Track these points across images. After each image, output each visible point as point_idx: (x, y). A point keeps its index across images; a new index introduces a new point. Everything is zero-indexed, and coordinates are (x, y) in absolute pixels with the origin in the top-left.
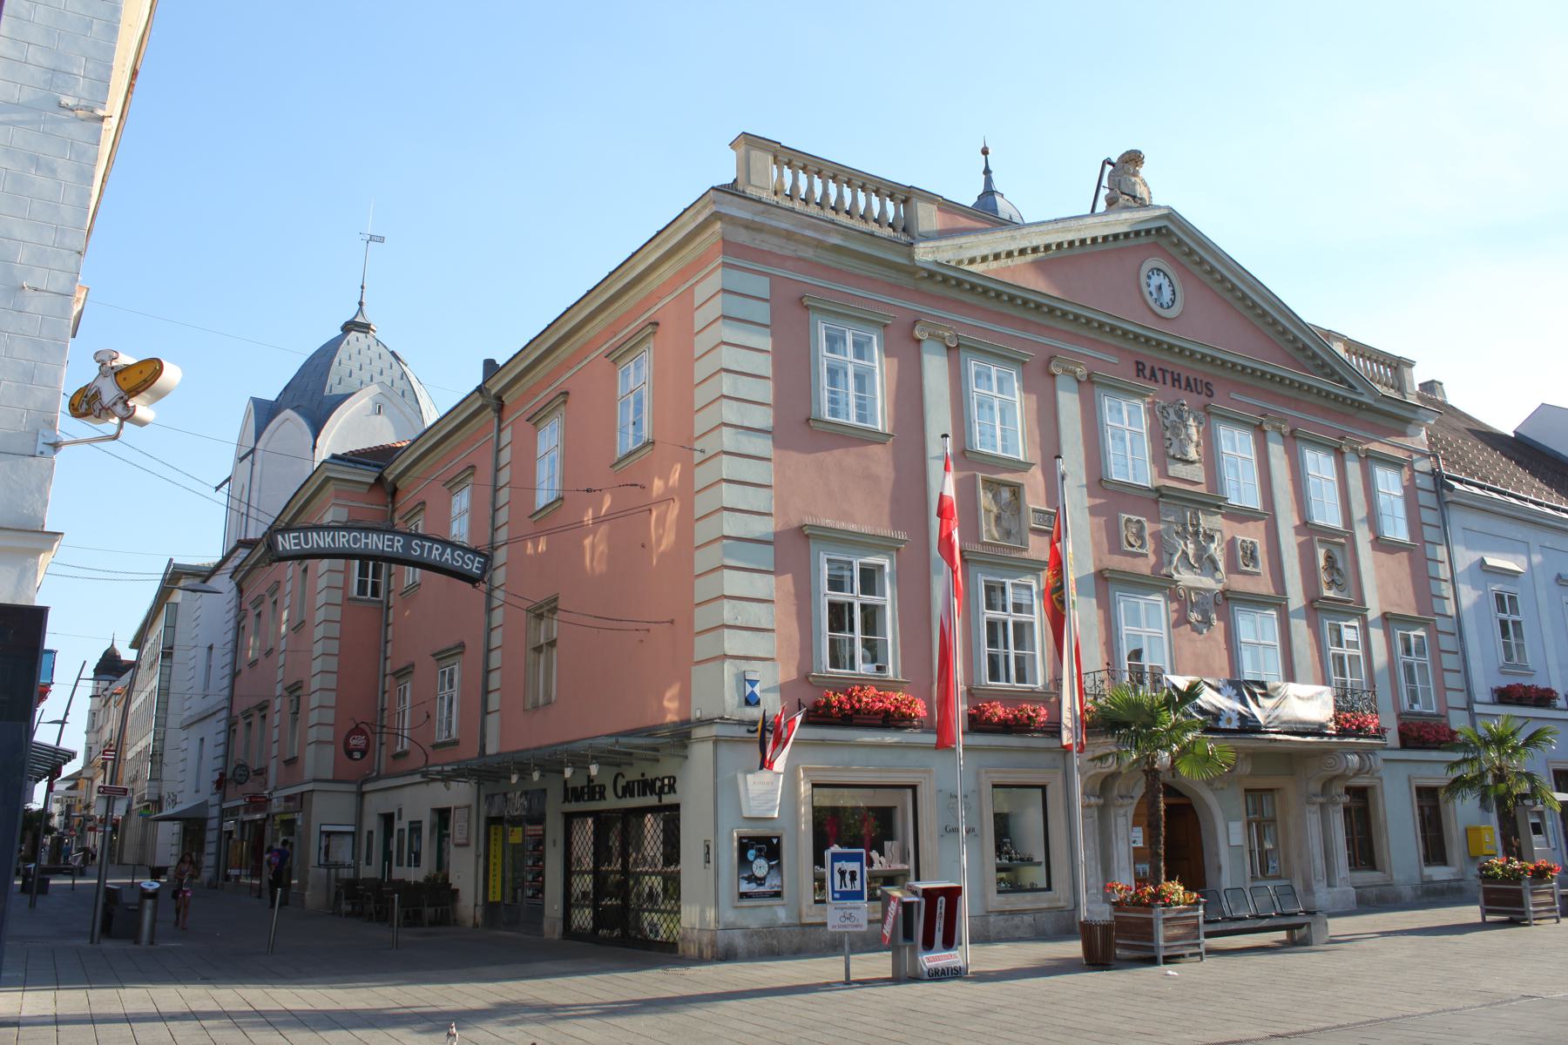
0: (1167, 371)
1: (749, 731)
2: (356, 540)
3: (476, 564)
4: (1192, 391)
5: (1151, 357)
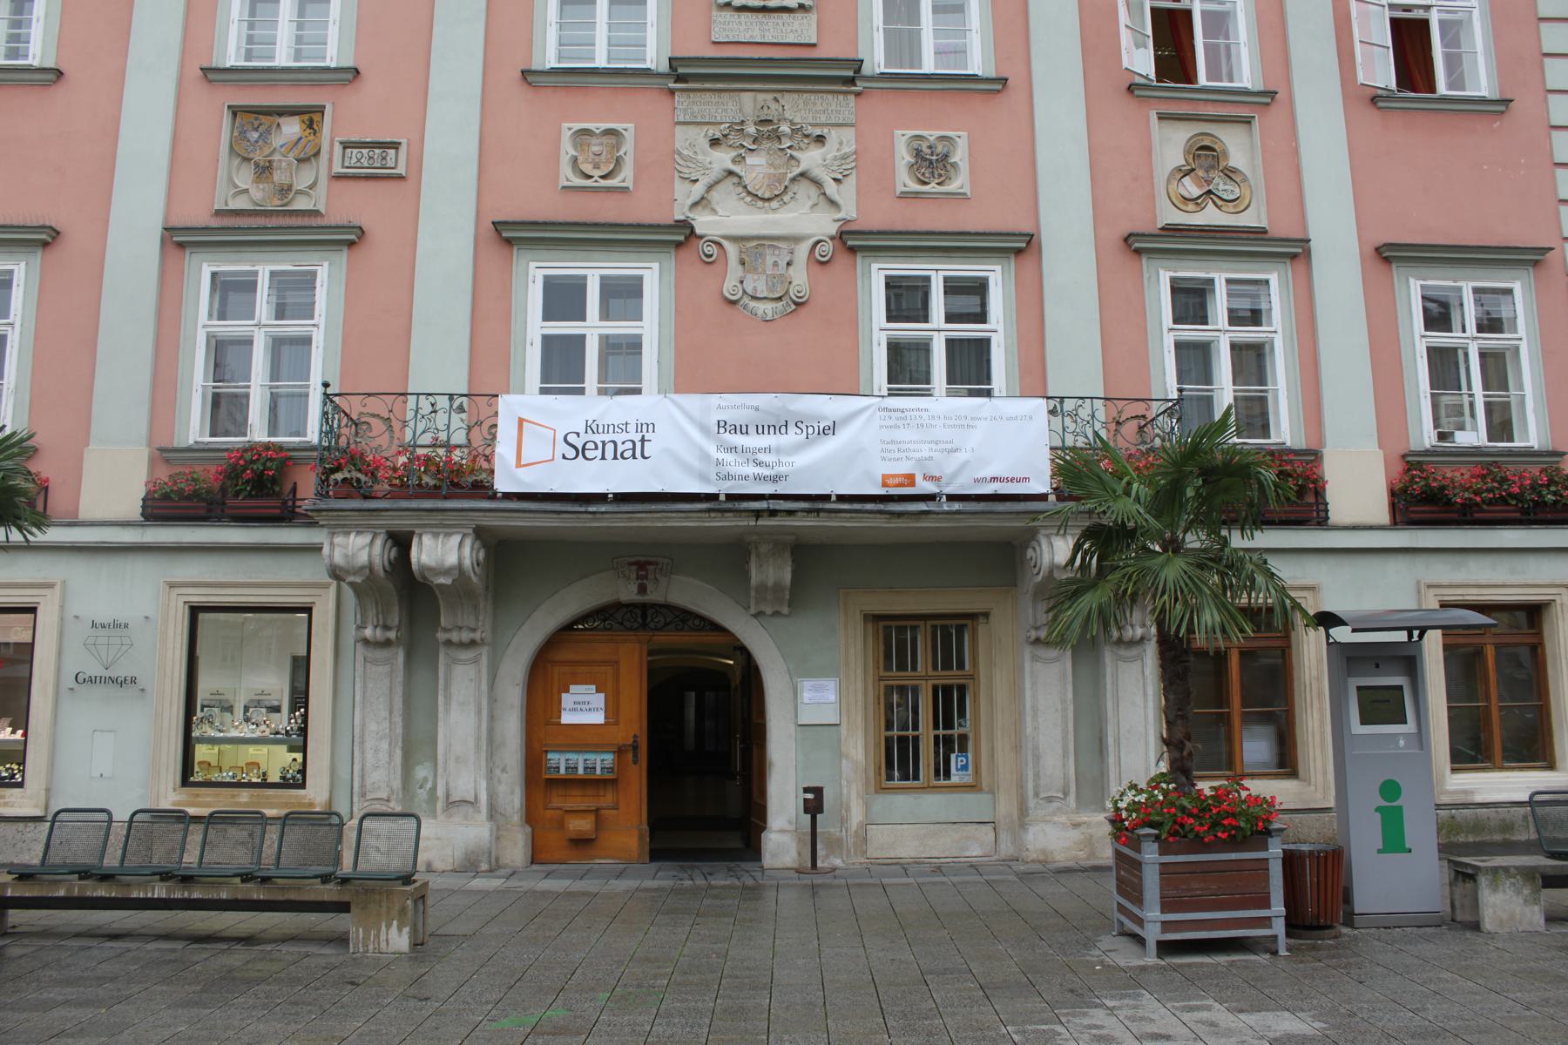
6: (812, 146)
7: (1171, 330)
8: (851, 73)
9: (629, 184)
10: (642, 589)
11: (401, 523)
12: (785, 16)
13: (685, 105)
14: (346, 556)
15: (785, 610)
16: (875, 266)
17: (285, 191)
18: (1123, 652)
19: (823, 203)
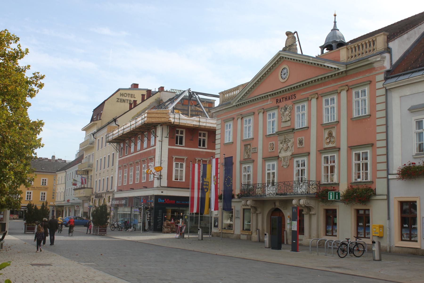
0: (284, 98)
5: (279, 96)
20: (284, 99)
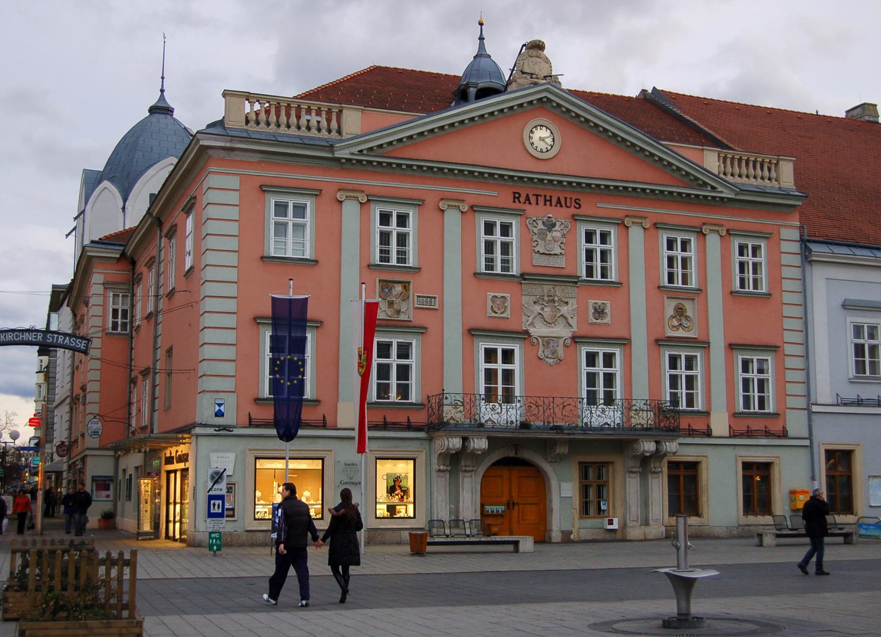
0: (541, 195)
1: (215, 430)
2: (17, 336)
3: (83, 344)
4: (561, 206)
6: (564, 305)
7: (668, 372)
8: (576, 280)
9: (509, 316)
10: (516, 453)
11: (466, 434)
12: (555, 256)
13: (527, 287)
14: (453, 445)
15: (558, 461)
16: (582, 348)
17: (398, 312)
18: (655, 476)
19: (567, 325)
20: (541, 200)
